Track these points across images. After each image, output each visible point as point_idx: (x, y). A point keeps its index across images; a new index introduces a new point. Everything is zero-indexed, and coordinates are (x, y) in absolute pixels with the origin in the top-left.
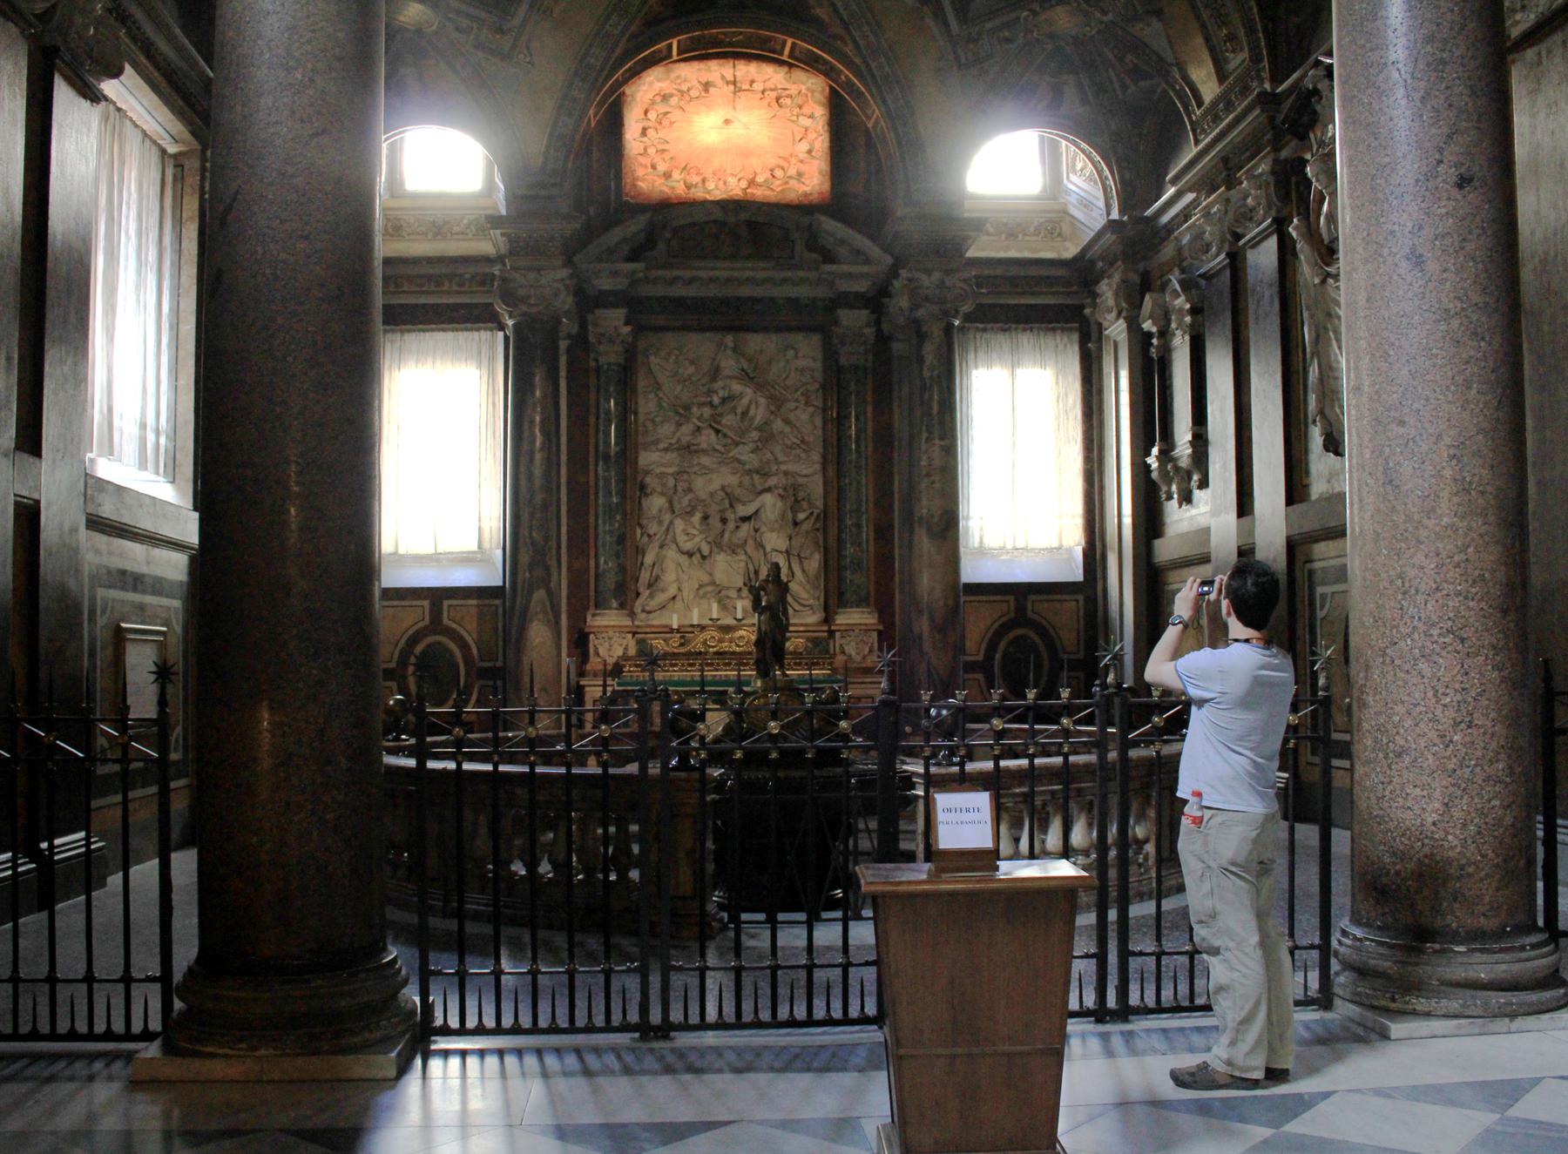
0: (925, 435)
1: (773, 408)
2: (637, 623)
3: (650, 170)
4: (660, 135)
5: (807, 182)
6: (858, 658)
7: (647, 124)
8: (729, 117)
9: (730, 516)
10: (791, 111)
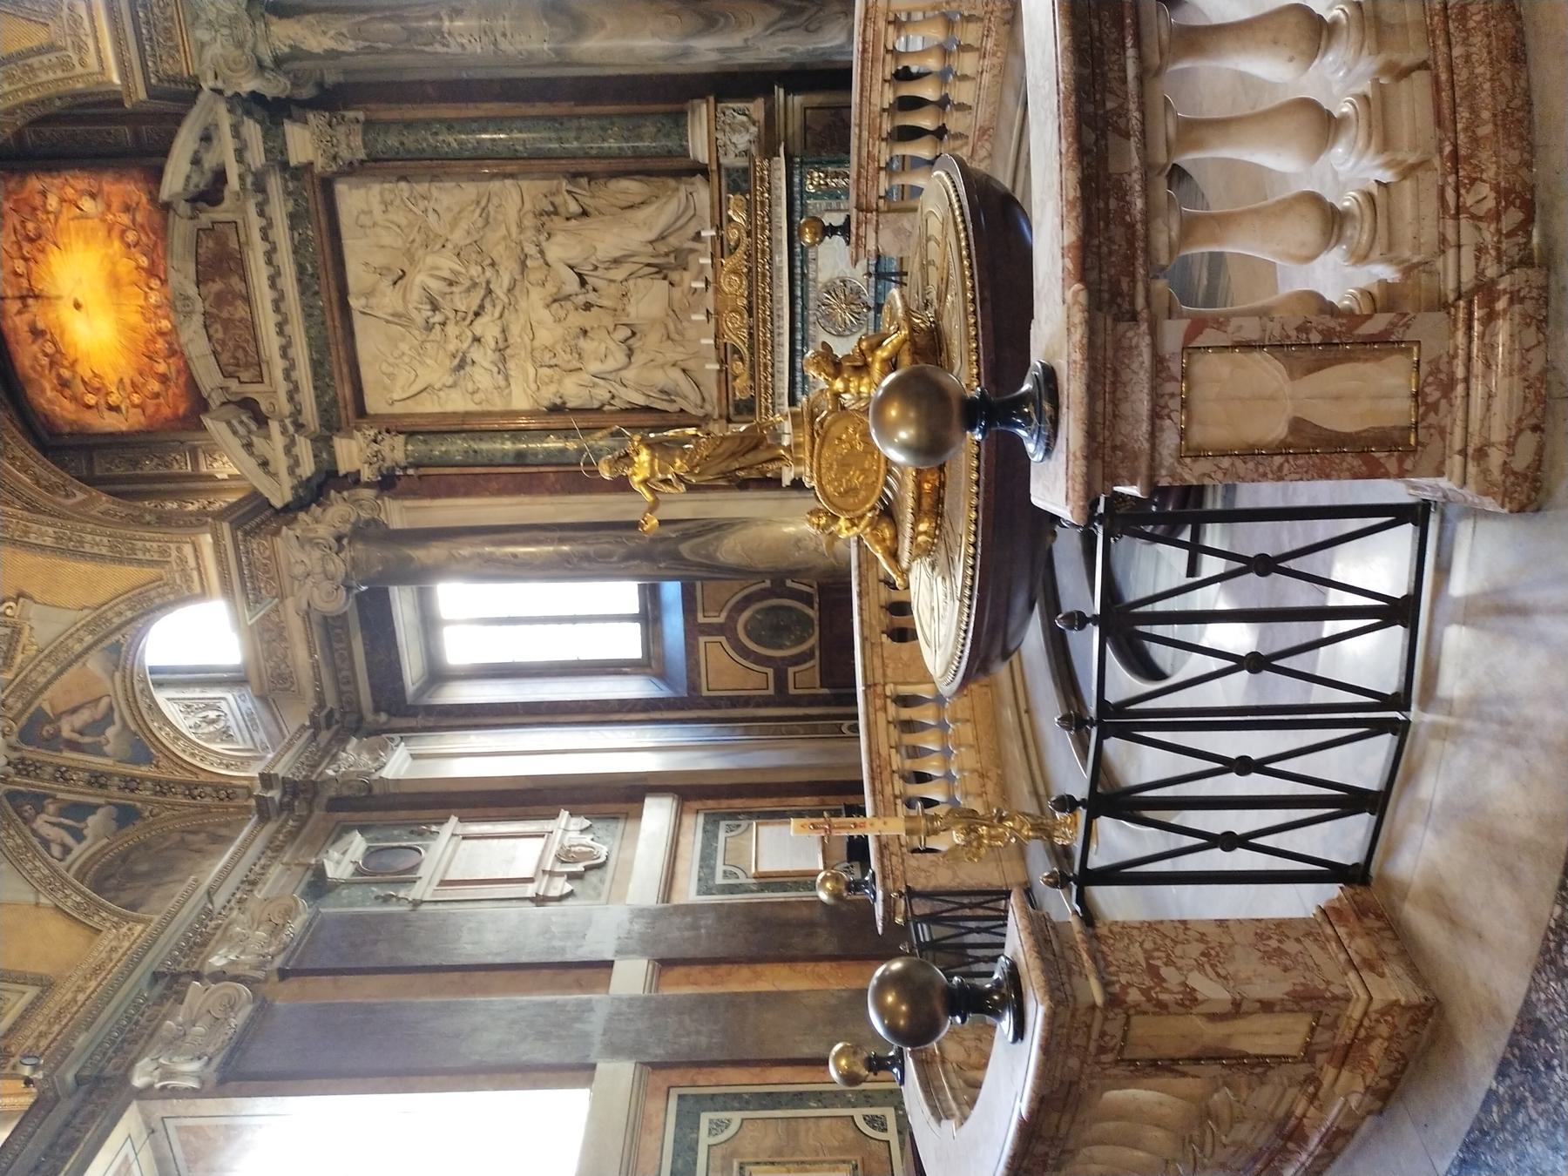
0: (439, 48)
1: (438, 246)
2: (716, 416)
3: (162, 400)
4: (113, 389)
5: (135, 198)
6: (754, 129)
7: (103, 406)
8: (71, 304)
9: (581, 299)
10: (44, 222)
